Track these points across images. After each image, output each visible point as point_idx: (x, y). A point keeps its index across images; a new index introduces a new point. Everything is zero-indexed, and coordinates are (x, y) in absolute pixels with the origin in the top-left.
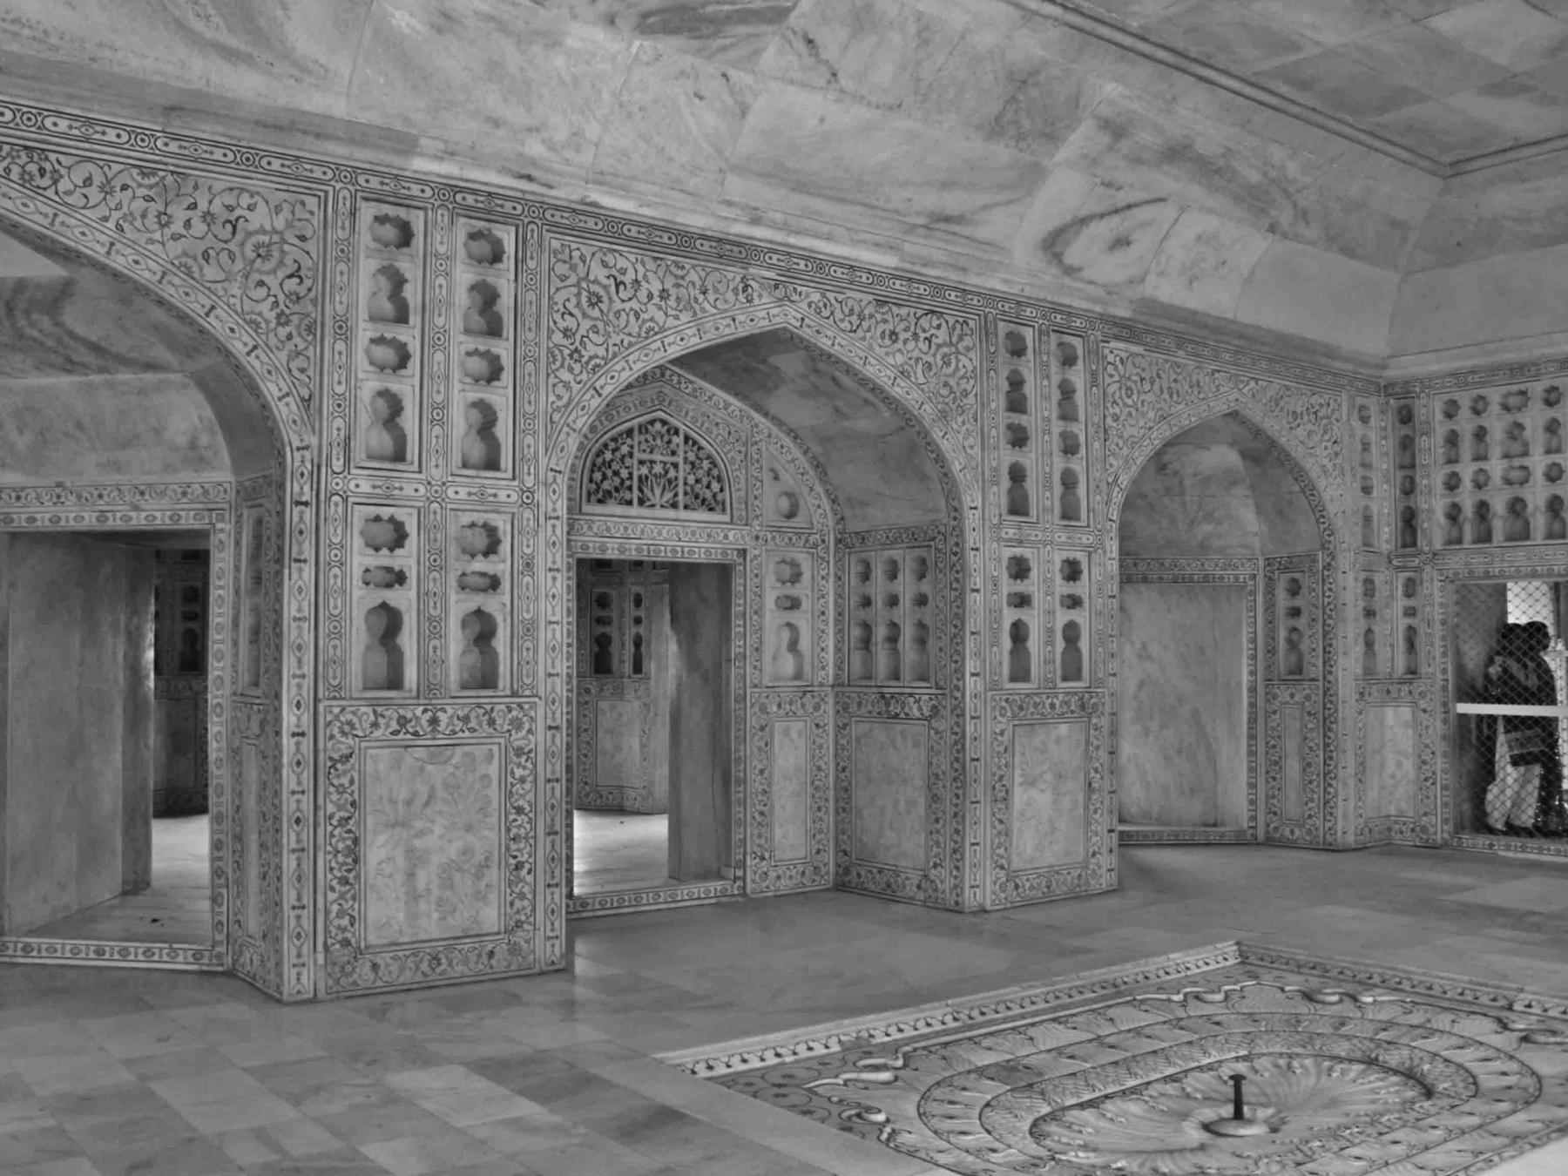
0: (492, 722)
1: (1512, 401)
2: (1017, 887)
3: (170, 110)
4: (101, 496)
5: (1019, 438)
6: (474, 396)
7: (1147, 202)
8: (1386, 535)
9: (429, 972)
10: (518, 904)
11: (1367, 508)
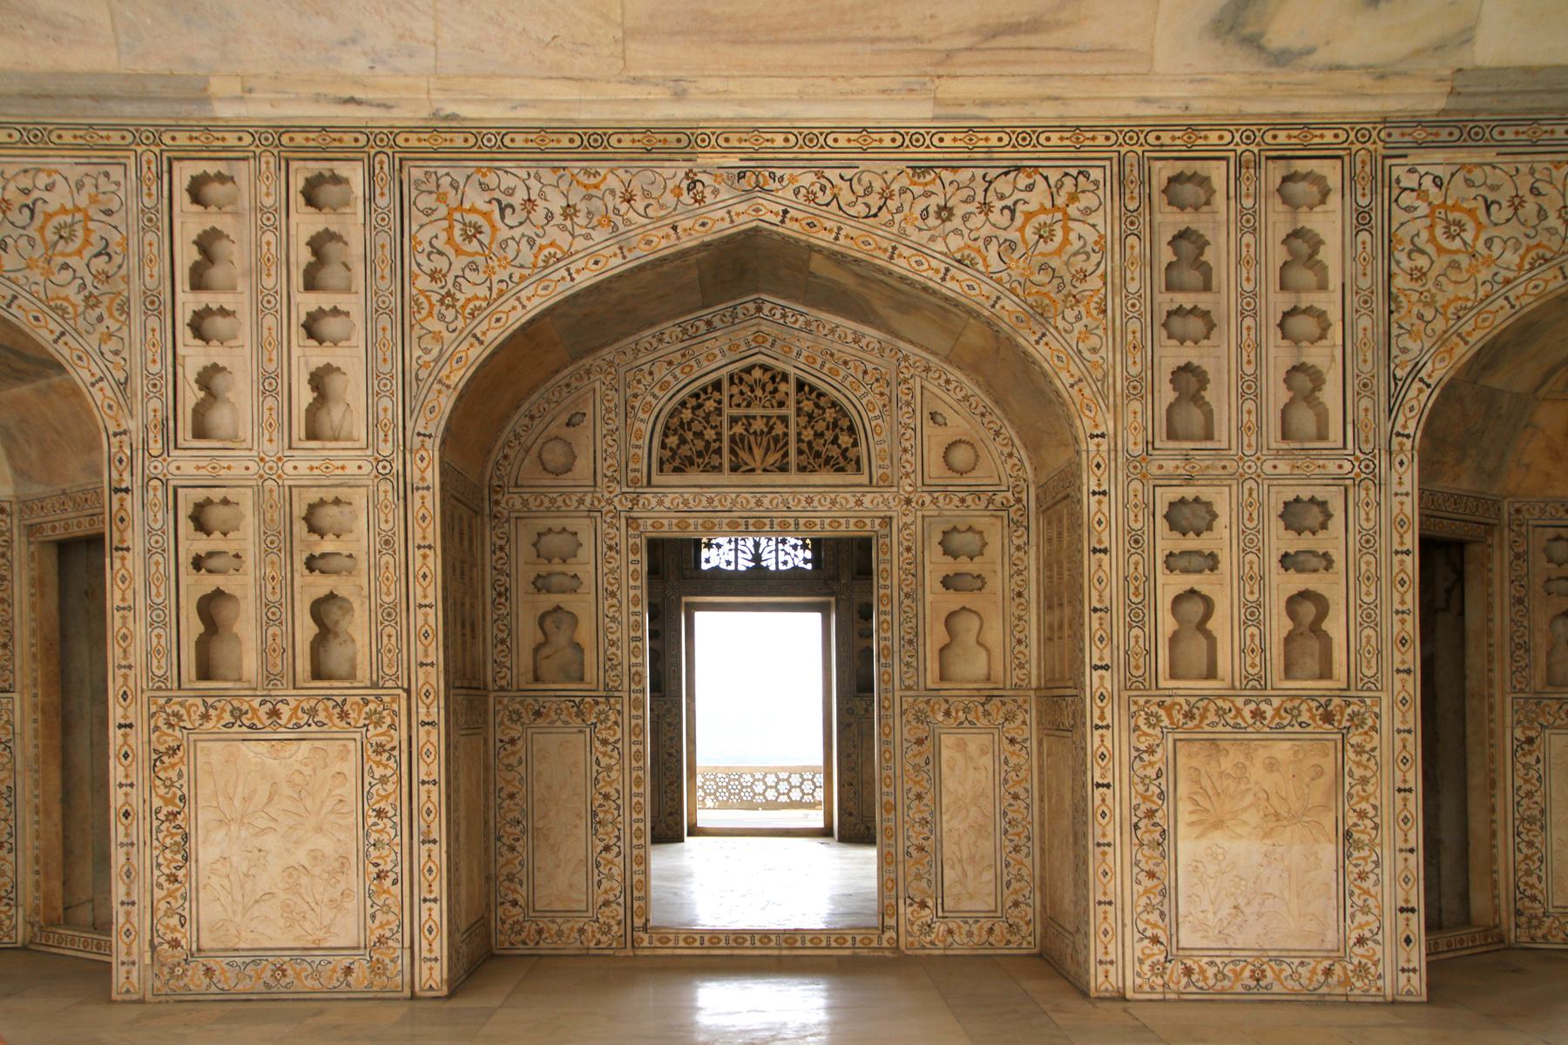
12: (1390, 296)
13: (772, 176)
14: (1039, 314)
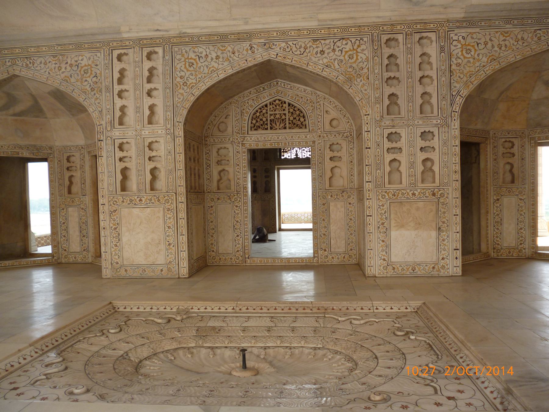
0: (159, 201)
2: (394, 268)
10: (170, 256)
13: (273, 44)
14: (350, 80)
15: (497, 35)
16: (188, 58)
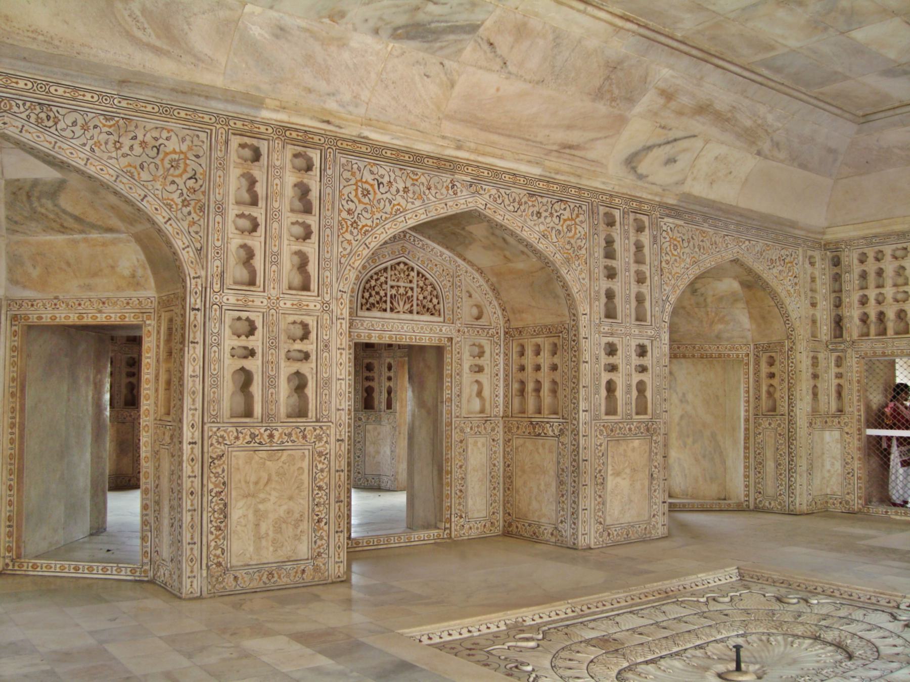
0: (304, 437)
1: (899, 253)
2: (609, 534)
3: (123, 82)
4: (80, 305)
5: (611, 274)
6: (296, 248)
7: (685, 138)
8: (825, 331)
9: (267, 581)
10: (319, 543)
11: (813, 315)
12: (661, 270)
14: (568, 261)
15: (697, 232)
16: (361, 180)
